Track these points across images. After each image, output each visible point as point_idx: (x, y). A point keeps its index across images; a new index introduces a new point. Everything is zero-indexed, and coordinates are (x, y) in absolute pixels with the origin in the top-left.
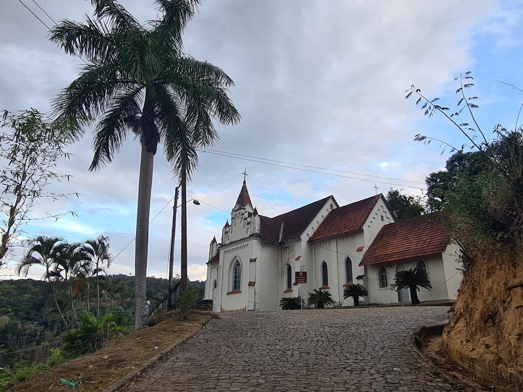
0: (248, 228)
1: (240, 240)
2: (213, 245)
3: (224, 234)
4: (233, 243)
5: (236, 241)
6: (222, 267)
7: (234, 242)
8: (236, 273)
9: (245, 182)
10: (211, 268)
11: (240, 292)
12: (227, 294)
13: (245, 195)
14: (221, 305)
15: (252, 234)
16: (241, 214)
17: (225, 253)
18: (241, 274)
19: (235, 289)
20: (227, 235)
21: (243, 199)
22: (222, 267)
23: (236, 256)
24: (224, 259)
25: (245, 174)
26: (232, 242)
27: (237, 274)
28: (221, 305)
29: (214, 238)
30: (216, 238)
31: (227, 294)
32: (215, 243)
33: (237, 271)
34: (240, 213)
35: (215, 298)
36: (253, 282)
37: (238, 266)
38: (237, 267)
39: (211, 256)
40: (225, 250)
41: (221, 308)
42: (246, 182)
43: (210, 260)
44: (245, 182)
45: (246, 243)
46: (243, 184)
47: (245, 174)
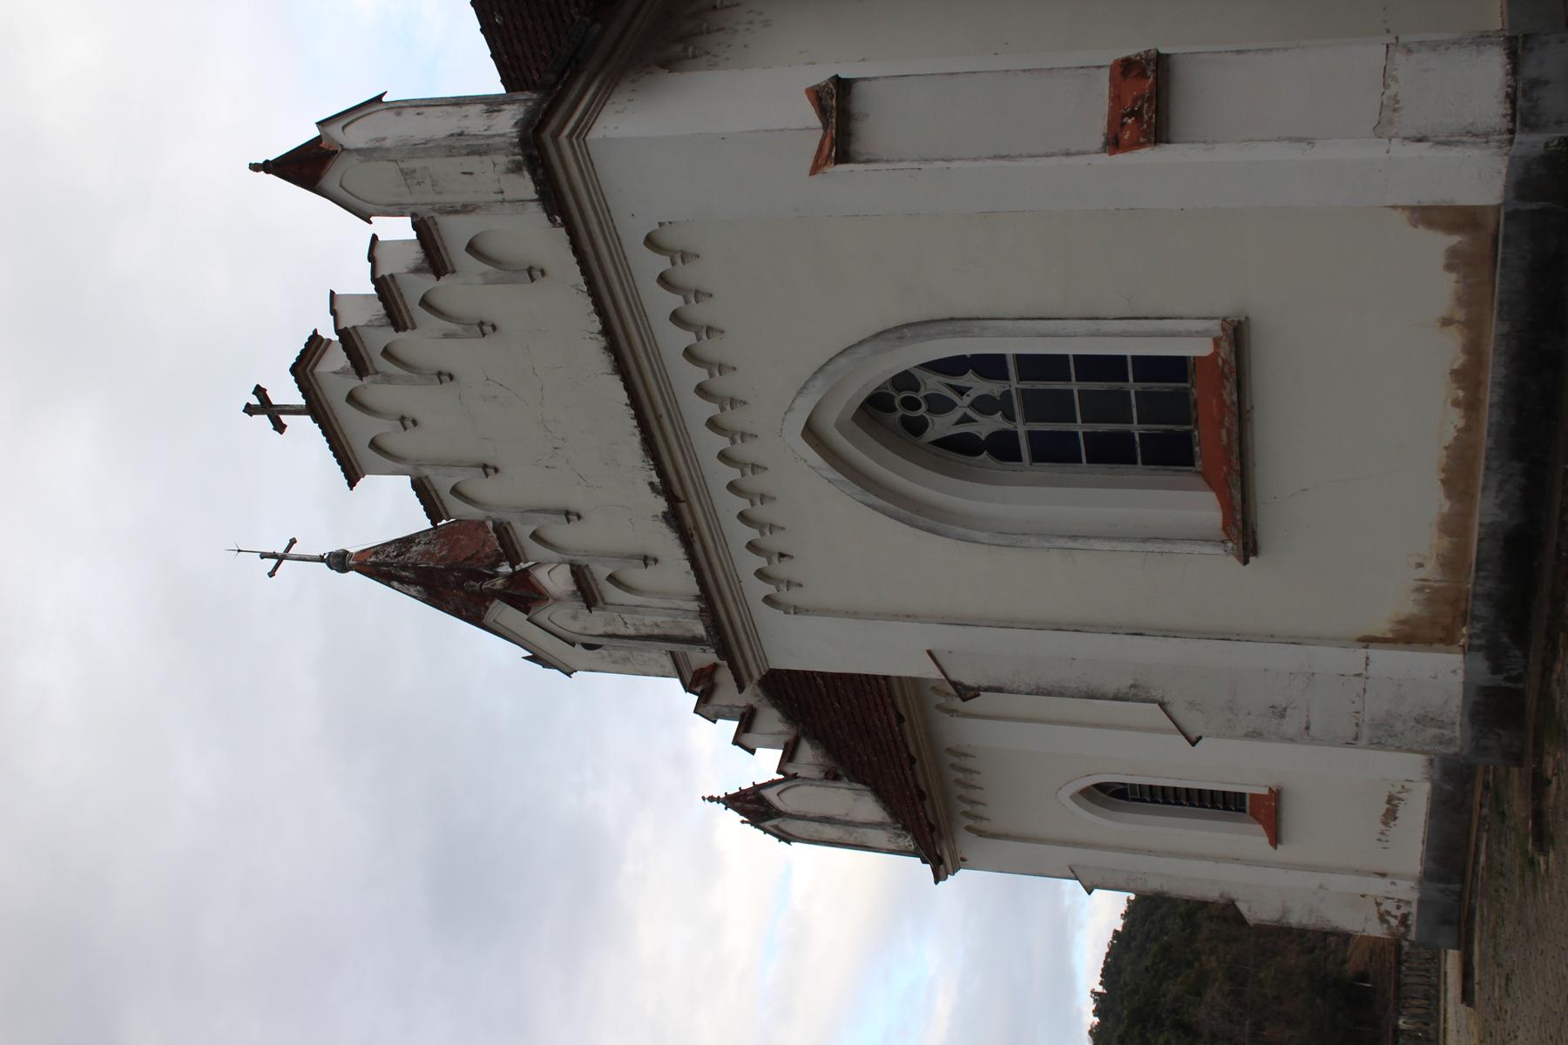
0: (472, 248)
1: (621, 368)
2: (779, 814)
3: (596, 622)
4: (666, 488)
5: (650, 445)
6: (944, 638)
7: (661, 472)
8: (1003, 448)
9: (339, 561)
10: (981, 834)
11: (1237, 333)
12: (1248, 548)
13: (423, 554)
14: (1368, 641)
15: (525, 186)
16: (353, 382)
17: (787, 596)
18: (1010, 346)
19: (1190, 462)
20: (600, 571)
21: (450, 569)
22: (944, 638)
23: (811, 433)
24: (854, 614)
25: (280, 558)
26: (661, 505)
27: (1022, 428)
28: (1368, 641)
29: (733, 801)
30: (733, 790)
31: (1248, 548)
32: (770, 794)
33: (985, 426)
34: (352, 398)
35: (1282, 714)
36: (1116, 99)
37: (916, 428)
38: (942, 426)
39: (880, 837)
40: (756, 590)
41: (1407, 636)
42: (335, 547)
43: (907, 842)
44: (339, 561)
45: (647, 266)
46: (353, 574)
47: (280, 558)
